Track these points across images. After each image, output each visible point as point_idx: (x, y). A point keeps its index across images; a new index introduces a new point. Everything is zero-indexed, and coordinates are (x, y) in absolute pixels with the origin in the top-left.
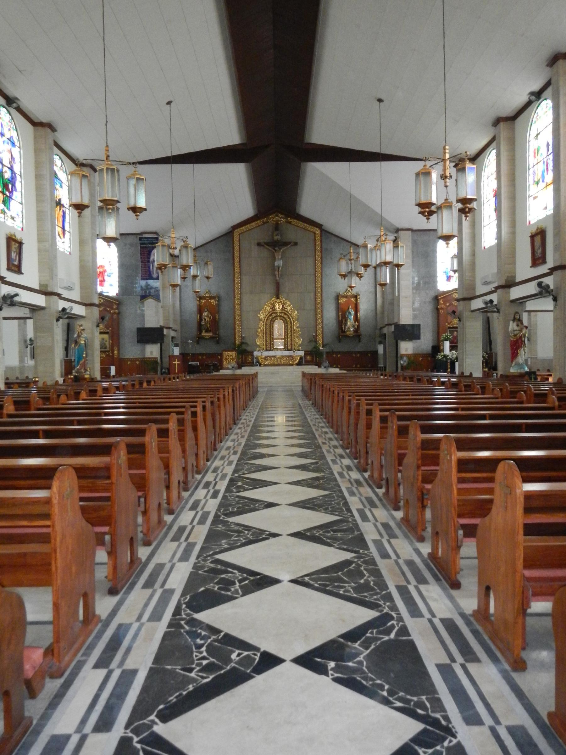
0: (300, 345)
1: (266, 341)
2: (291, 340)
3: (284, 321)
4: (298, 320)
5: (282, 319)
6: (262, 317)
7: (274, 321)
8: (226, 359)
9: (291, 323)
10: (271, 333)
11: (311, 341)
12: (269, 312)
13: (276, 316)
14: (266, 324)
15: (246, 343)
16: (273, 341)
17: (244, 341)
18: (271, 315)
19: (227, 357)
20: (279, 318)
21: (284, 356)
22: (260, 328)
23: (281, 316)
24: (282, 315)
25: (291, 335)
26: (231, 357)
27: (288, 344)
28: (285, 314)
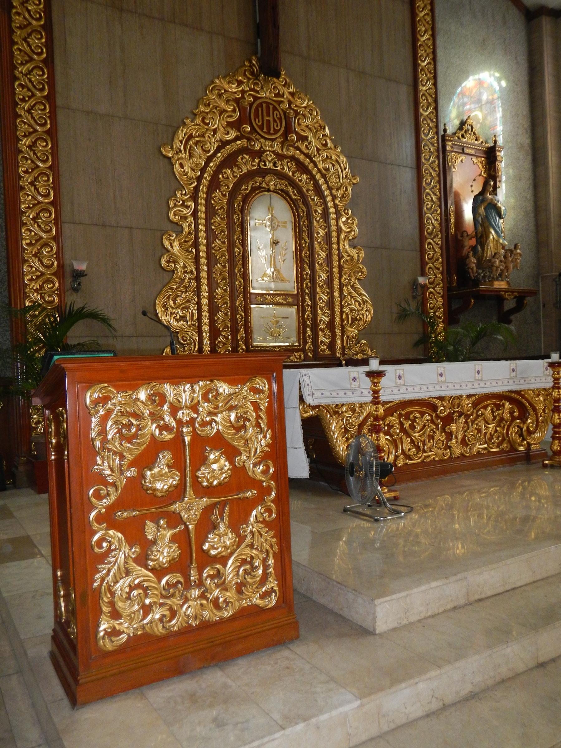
0: (369, 332)
1: (213, 310)
2: (330, 304)
3: (293, 205)
4: (353, 204)
5: (284, 194)
6: (186, 168)
7: (246, 199)
8: (139, 507)
9: (325, 215)
10: (238, 262)
11: (403, 315)
12: (224, 144)
13: (262, 172)
14: (210, 212)
15: (93, 316)
16: (247, 310)
17: (76, 301)
18: (230, 161)
19: (161, 478)
20: (272, 182)
21: (480, 401)
22: (179, 229)
23: (281, 176)
24: (288, 168)
25: (329, 283)
26: (217, 467)
27: (315, 327)
28: (302, 168)
